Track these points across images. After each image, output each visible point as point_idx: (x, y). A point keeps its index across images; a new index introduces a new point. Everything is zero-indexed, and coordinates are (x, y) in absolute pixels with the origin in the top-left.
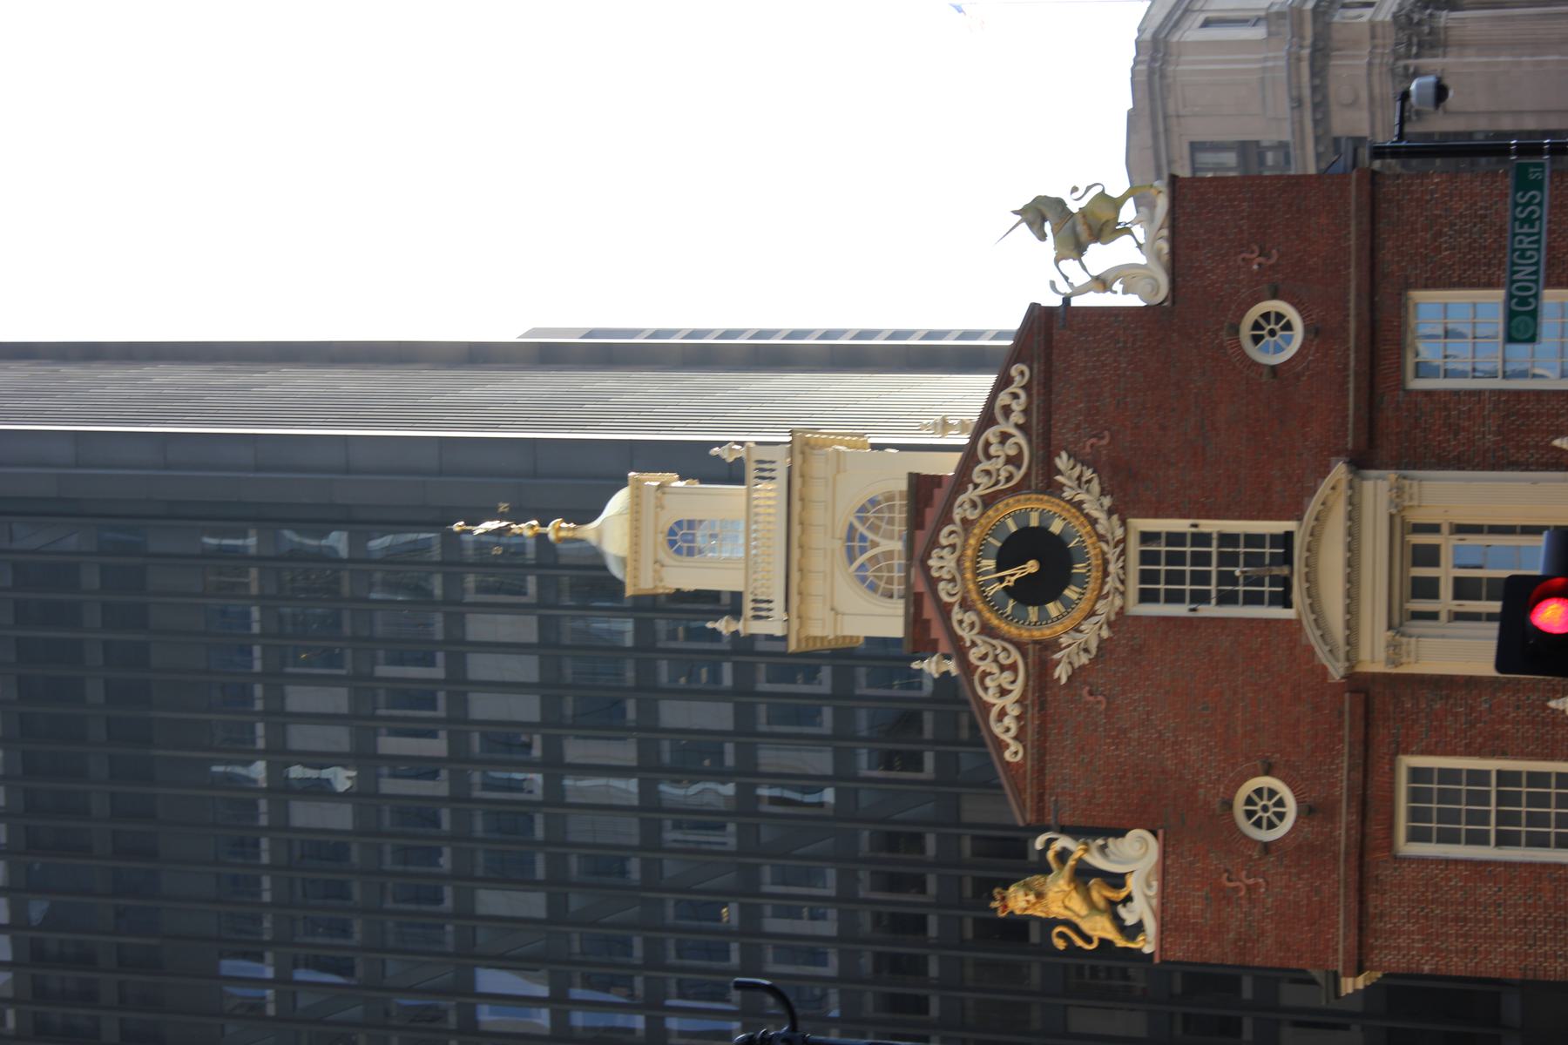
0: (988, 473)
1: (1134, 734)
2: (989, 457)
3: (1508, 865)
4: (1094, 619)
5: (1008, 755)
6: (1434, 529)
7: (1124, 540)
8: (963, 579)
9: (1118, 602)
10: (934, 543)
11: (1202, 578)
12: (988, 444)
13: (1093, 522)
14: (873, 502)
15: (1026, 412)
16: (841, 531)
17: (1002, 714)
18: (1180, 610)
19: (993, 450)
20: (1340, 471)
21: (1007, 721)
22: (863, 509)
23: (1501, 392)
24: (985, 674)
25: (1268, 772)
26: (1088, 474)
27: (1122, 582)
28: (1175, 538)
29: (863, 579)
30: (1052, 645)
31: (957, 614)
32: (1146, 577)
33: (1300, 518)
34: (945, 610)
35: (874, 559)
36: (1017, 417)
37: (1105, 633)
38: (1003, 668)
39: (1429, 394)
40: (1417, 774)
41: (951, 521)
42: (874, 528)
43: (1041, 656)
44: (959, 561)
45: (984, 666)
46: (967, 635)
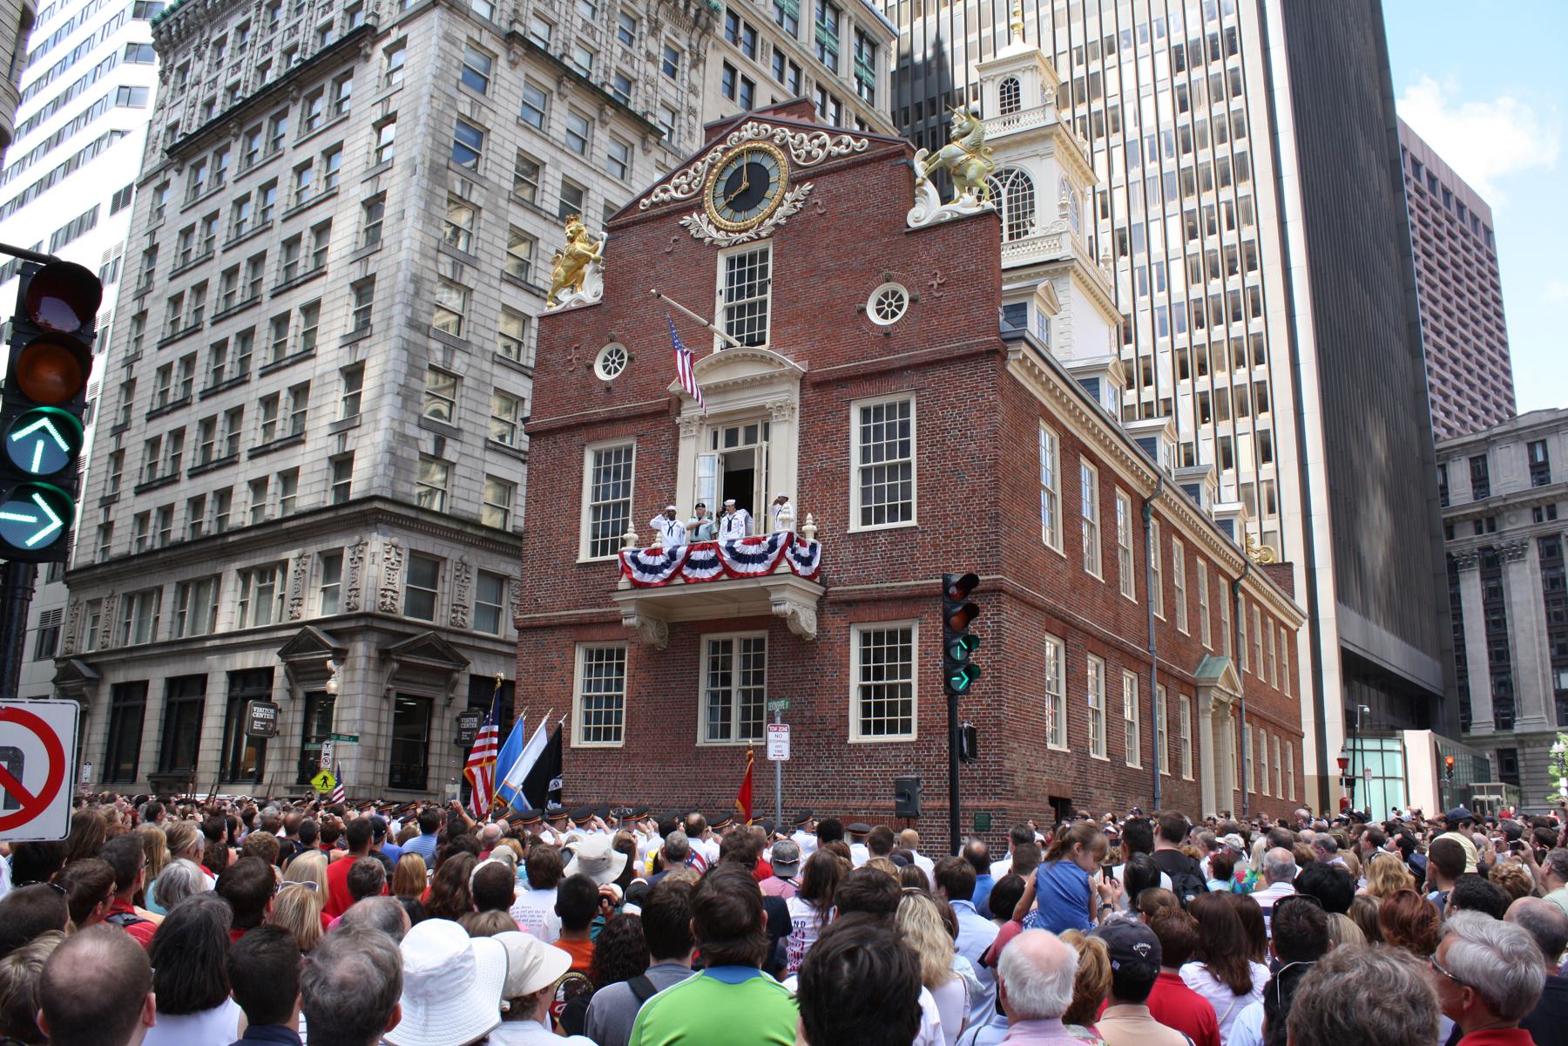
0: (802, 142)
1: (652, 273)
2: (810, 141)
3: (579, 514)
4: (714, 234)
5: (644, 200)
6: (766, 438)
7: (760, 238)
8: (738, 146)
9: (724, 244)
10: (761, 121)
11: (740, 295)
12: (818, 137)
13: (770, 216)
14: (1028, 180)
15: (840, 155)
16: (1010, 166)
17: (665, 191)
18: (721, 283)
19: (816, 142)
20: (802, 367)
21: (661, 195)
22: (1023, 175)
23: (848, 467)
24: (686, 174)
25: (630, 359)
26: (799, 205)
27: (735, 244)
28: (764, 270)
30: (700, 208)
31: (720, 147)
32: (742, 260)
33: (771, 347)
34: (722, 140)
35: (996, 187)
36: (836, 150)
37: (707, 240)
38: (689, 184)
39: (847, 418)
40: (629, 451)
41: (773, 128)
42: (1013, 184)
43: (697, 206)
44: (750, 140)
45: (691, 172)
46: (708, 158)
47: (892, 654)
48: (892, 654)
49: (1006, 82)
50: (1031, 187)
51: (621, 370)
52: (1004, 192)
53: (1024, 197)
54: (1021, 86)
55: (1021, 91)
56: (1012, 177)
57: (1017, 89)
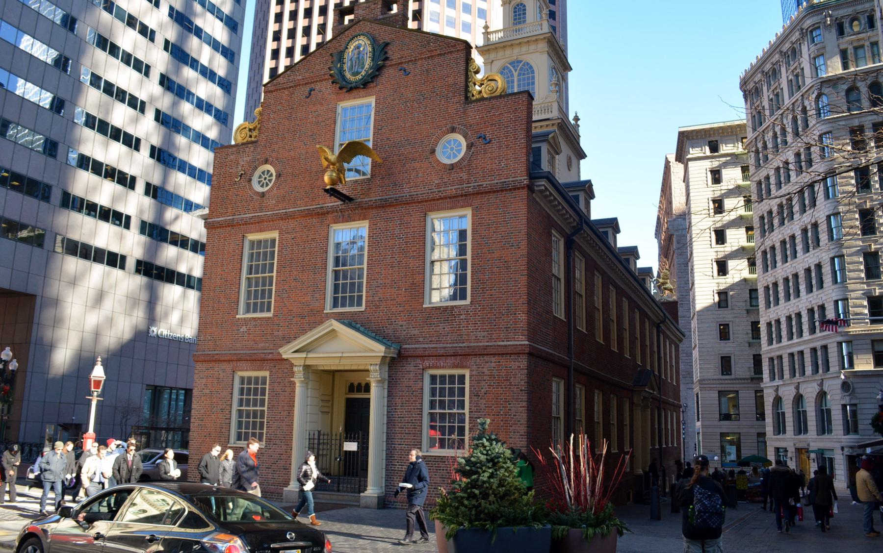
14: (531, 67)
16: (520, 58)
22: (528, 64)
29: (504, 69)
35: (510, 71)
42: (520, 70)
47: (452, 392)
48: (452, 392)
49: (518, 5)
50: (533, 72)
51: (270, 185)
52: (516, 74)
53: (528, 78)
54: (527, 8)
55: (527, 11)
56: (521, 64)
57: (525, 10)
